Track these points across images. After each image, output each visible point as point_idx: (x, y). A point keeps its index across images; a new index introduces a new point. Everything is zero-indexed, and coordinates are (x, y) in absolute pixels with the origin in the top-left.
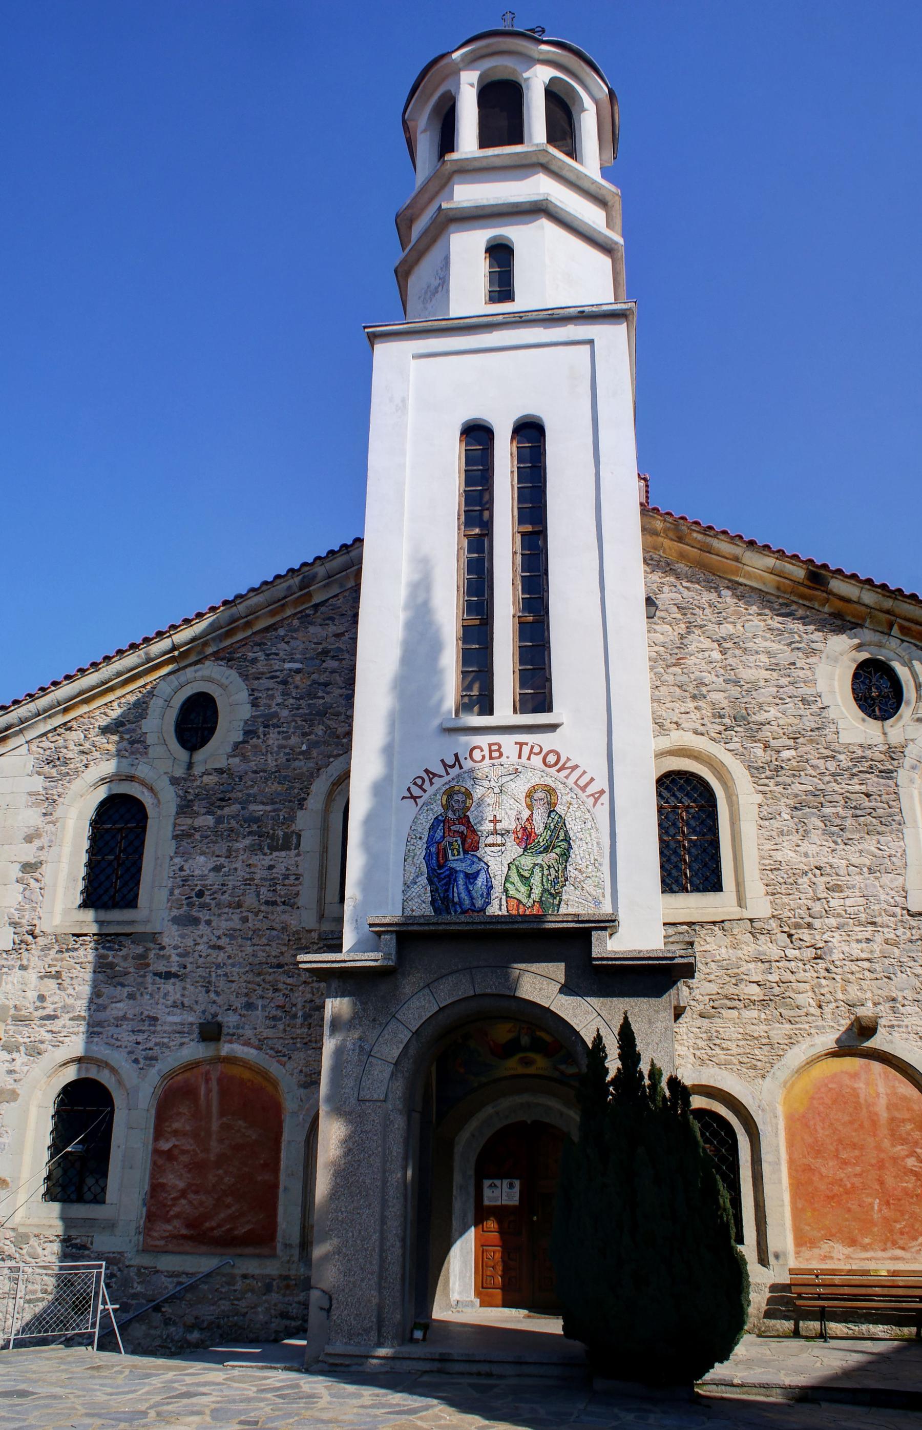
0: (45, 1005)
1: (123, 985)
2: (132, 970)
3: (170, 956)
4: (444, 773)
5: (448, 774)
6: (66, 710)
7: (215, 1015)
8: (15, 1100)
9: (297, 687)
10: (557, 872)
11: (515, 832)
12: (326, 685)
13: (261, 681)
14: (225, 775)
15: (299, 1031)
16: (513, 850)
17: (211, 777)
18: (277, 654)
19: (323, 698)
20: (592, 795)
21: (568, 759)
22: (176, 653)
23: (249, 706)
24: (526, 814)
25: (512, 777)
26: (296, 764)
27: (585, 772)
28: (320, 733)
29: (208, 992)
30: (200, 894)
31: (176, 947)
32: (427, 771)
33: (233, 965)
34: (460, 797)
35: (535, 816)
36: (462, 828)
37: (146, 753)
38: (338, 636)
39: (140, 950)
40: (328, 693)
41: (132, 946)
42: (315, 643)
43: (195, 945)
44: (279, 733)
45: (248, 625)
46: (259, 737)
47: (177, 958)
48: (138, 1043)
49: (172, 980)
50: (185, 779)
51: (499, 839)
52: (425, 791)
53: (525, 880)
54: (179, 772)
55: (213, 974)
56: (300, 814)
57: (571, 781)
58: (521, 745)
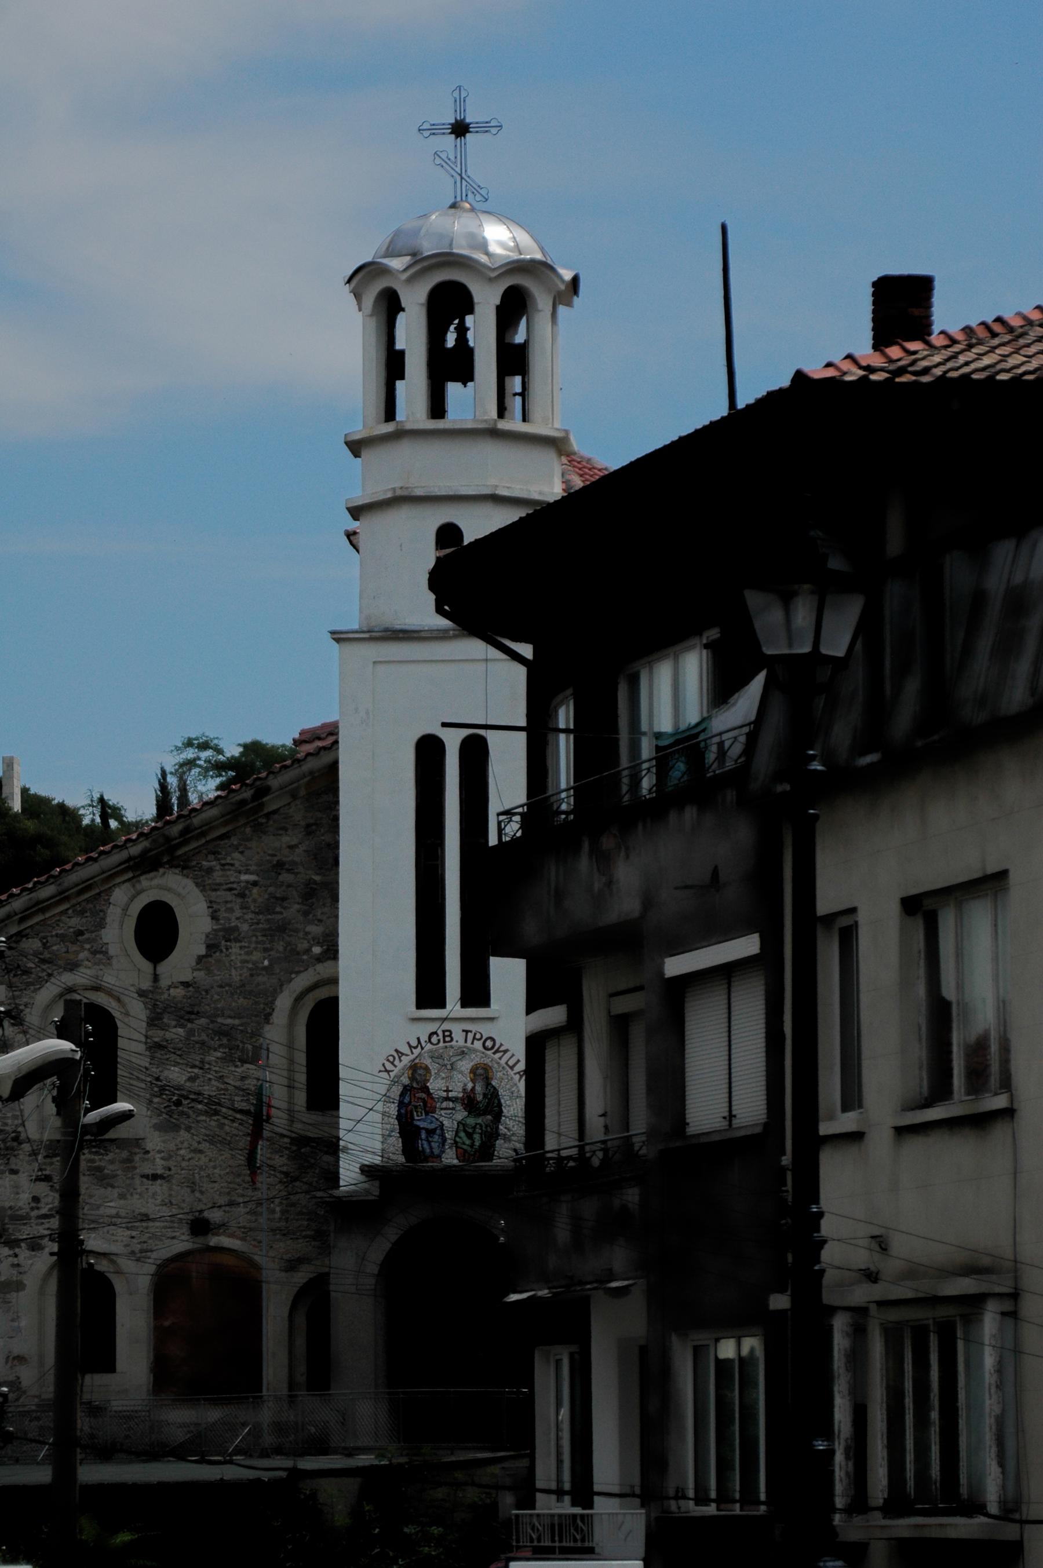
0: (39, 1205)
1: (113, 1187)
2: (119, 1172)
3: (154, 1159)
4: (409, 1053)
5: (412, 1053)
6: (22, 920)
7: (201, 1211)
8: (23, 1289)
9: (255, 901)
10: (492, 1129)
11: (462, 1099)
12: (284, 899)
13: (219, 893)
14: (191, 989)
15: (278, 1225)
16: (461, 1114)
17: (178, 990)
18: (232, 865)
19: (281, 913)
20: (519, 1073)
21: (501, 1045)
22: (131, 863)
23: (209, 919)
24: (470, 1085)
25: (460, 1057)
26: (260, 979)
27: (513, 1055)
28: (281, 949)
29: (193, 1191)
30: (178, 1103)
31: (159, 1152)
32: (396, 1051)
33: (215, 1167)
34: (421, 1072)
35: (476, 1088)
36: (424, 1095)
37: (110, 964)
38: (291, 847)
39: (125, 1154)
40: (285, 908)
41: (117, 1151)
42: (270, 855)
43: (178, 1149)
44: (241, 948)
45: (203, 834)
46: (221, 951)
47: (163, 1162)
48: (133, 1237)
49: (159, 1182)
50: (152, 992)
51: (451, 1105)
52: (395, 1066)
53: (470, 1136)
54: (146, 985)
55: (197, 1175)
56: (267, 1028)
57: (503, 1061)
58: (467, 1032)
